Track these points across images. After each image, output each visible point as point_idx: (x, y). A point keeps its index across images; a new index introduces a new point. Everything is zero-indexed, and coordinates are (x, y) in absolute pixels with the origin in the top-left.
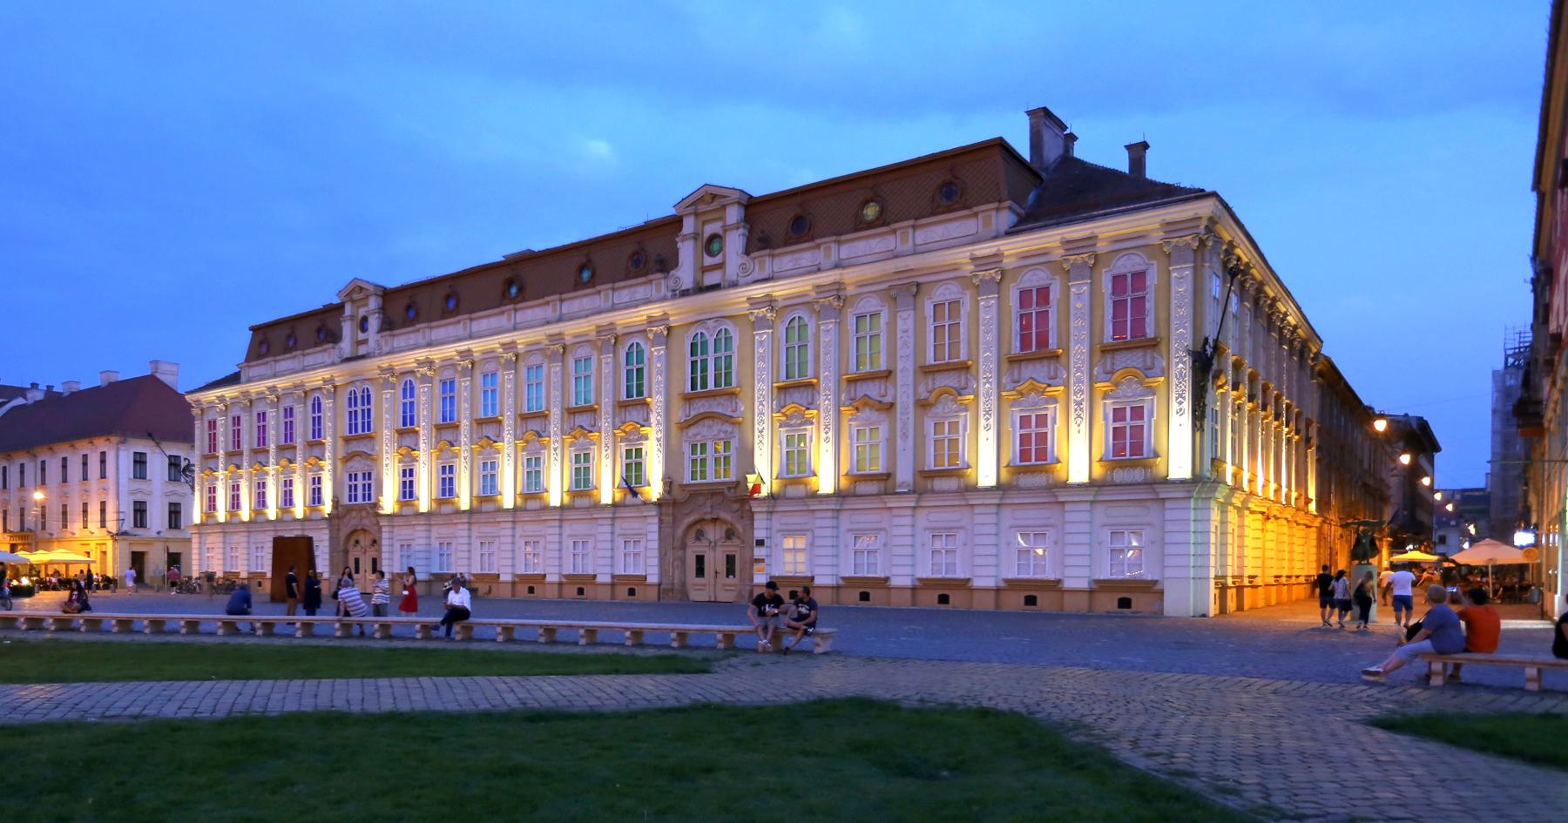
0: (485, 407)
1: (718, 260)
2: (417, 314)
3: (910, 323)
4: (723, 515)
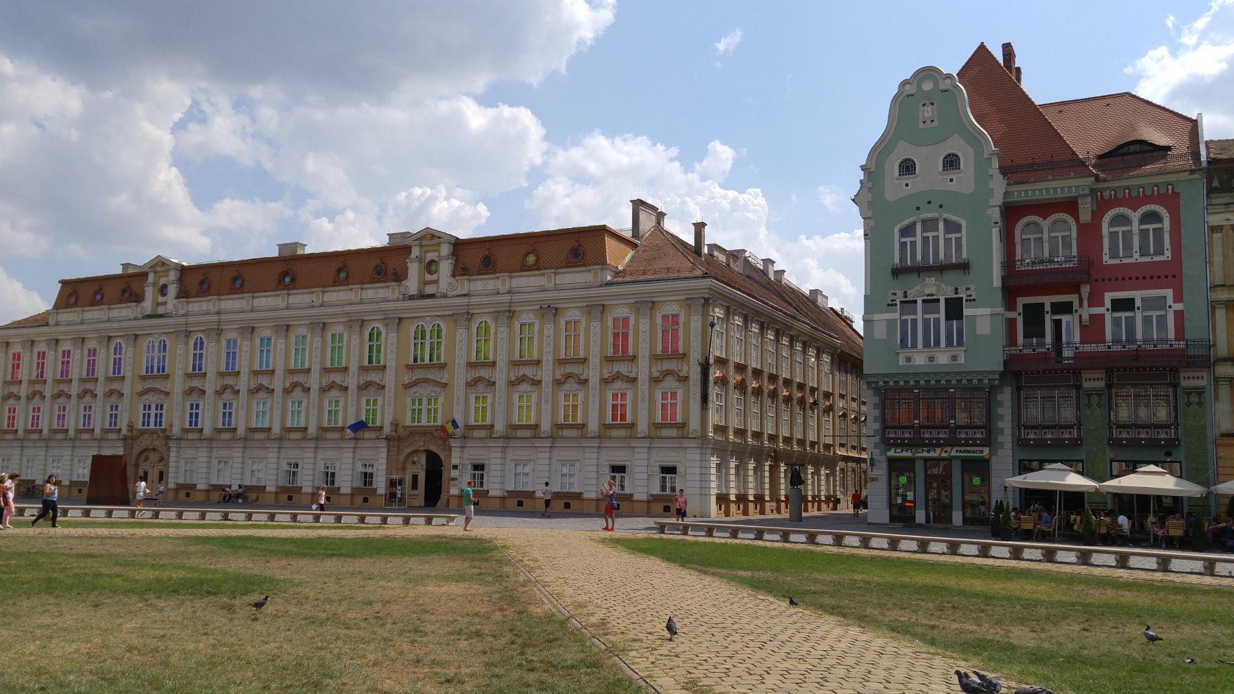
0: (261, 362)
1: (434, 277)
2: (209, 287)
3: (551, 331)
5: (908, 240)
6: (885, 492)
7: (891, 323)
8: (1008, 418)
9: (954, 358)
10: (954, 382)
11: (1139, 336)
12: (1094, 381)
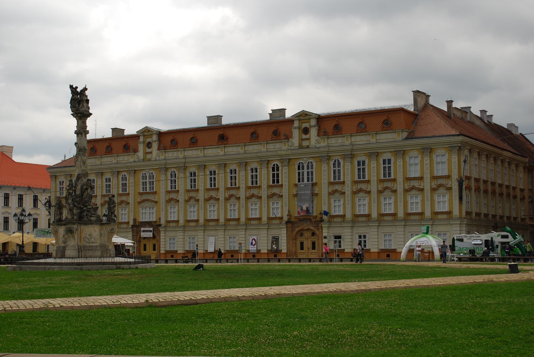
4: (311, 228)
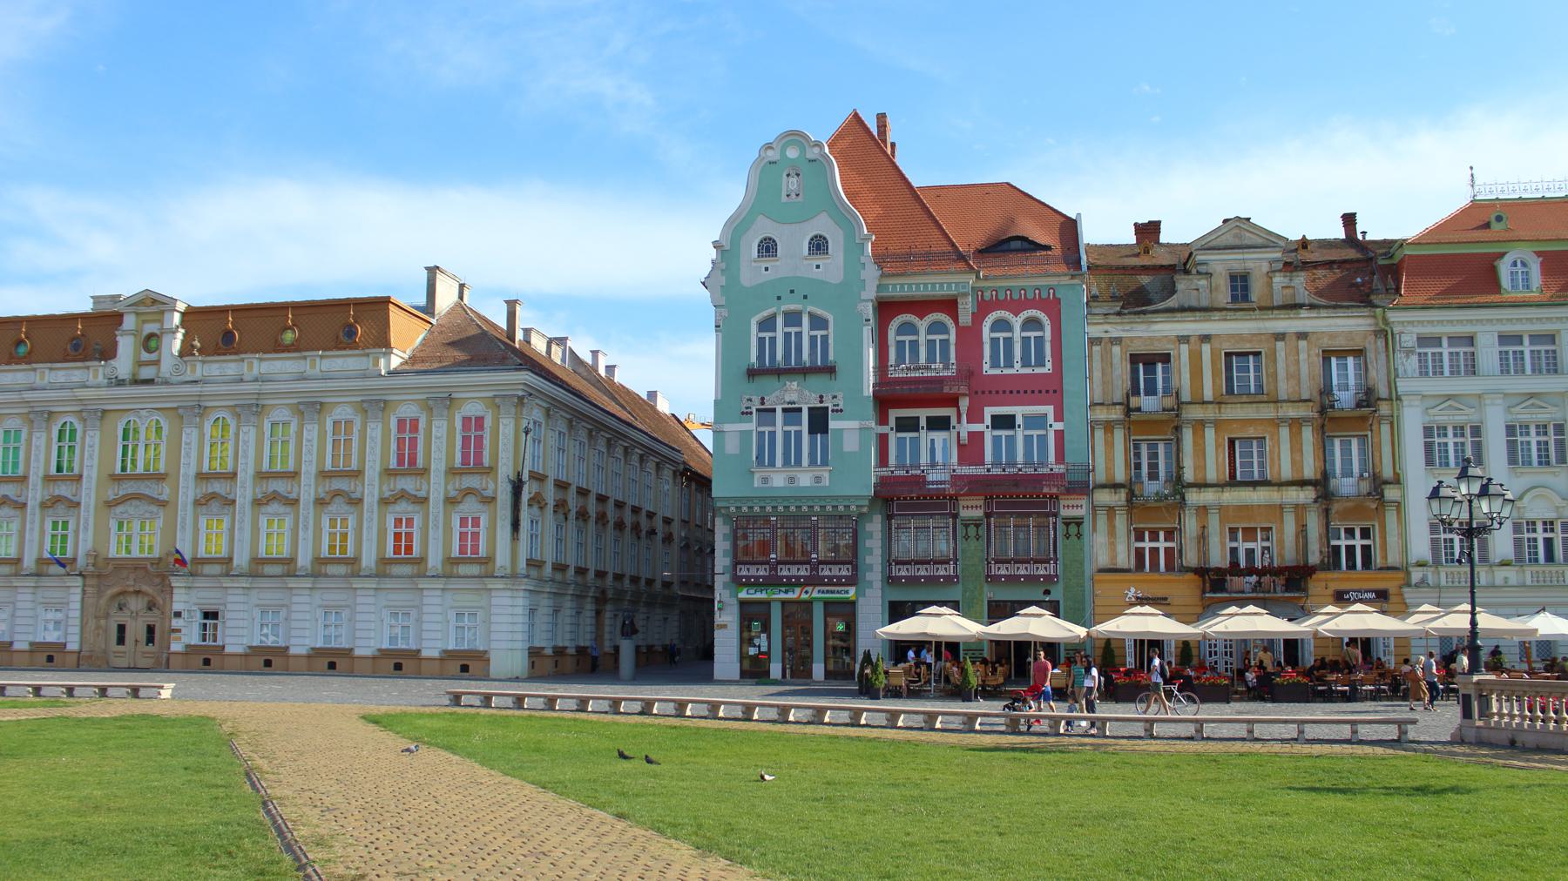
1: (153, 357)
4: (145, 588)
5: (767, 335)
6: (735, 642)
7: (745, 435)
8: (878, 552)
9: (818, 479)
10: (817, 508)
11: (1020, 458)
12: (971, 509)
